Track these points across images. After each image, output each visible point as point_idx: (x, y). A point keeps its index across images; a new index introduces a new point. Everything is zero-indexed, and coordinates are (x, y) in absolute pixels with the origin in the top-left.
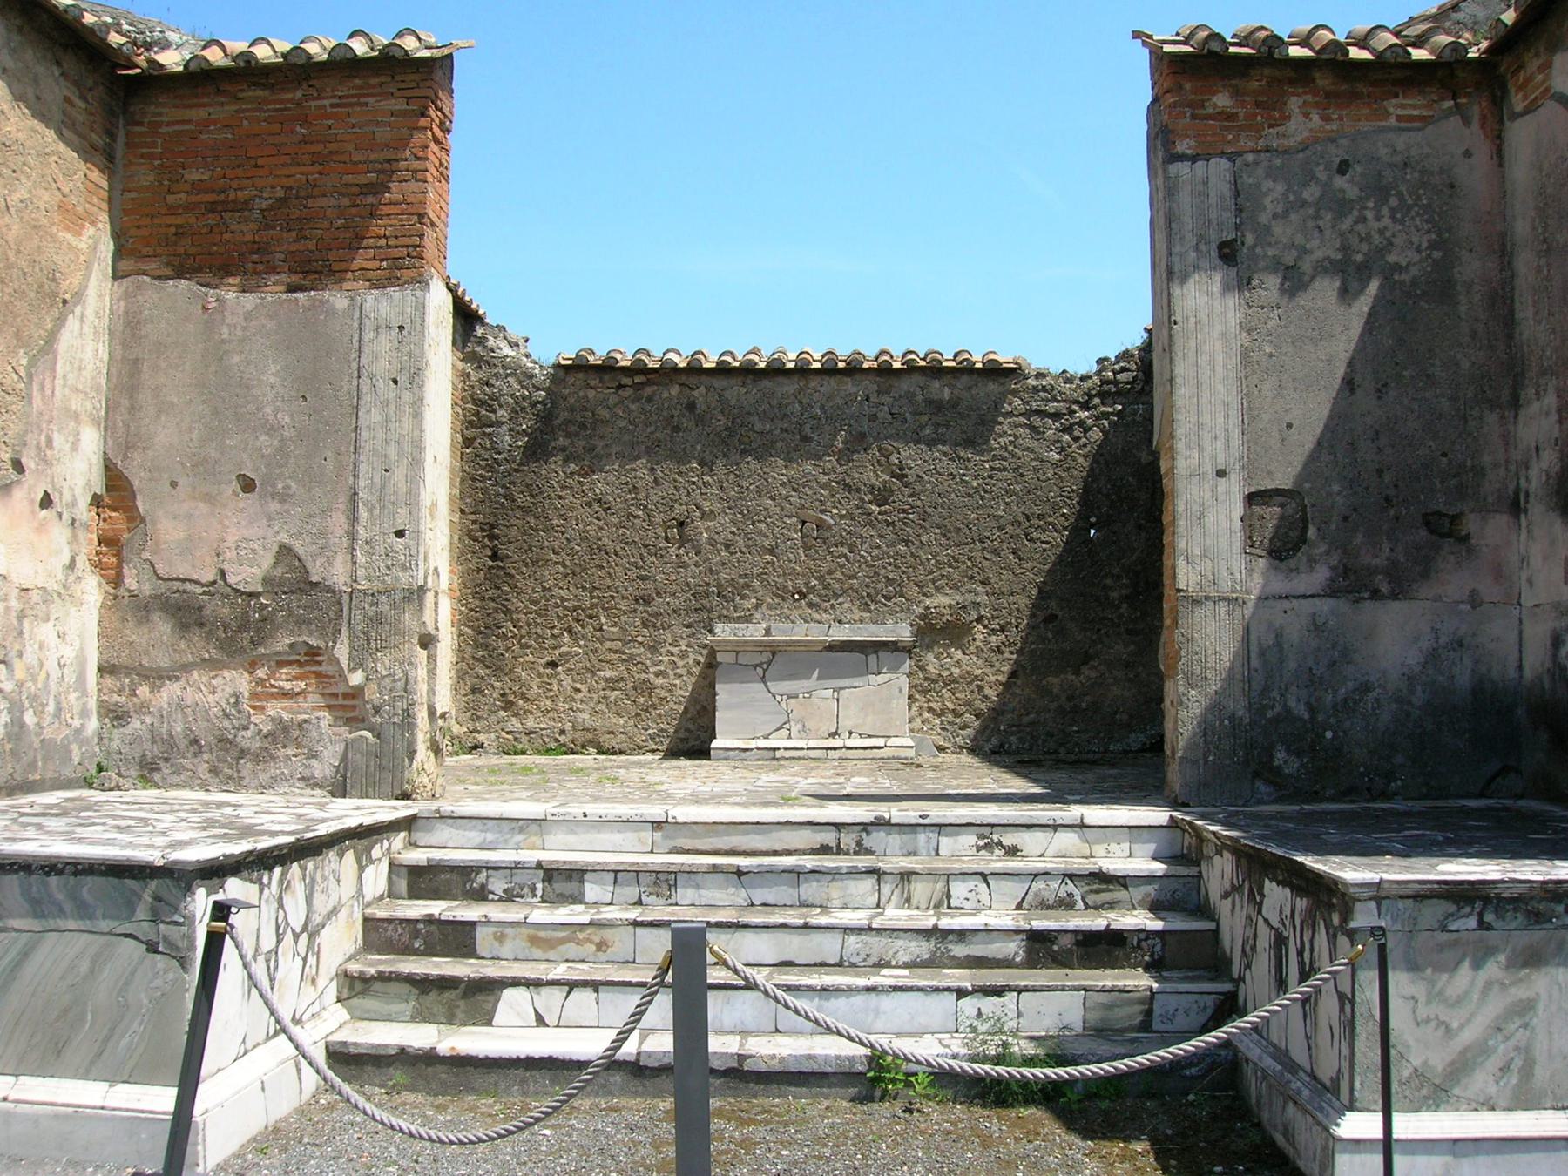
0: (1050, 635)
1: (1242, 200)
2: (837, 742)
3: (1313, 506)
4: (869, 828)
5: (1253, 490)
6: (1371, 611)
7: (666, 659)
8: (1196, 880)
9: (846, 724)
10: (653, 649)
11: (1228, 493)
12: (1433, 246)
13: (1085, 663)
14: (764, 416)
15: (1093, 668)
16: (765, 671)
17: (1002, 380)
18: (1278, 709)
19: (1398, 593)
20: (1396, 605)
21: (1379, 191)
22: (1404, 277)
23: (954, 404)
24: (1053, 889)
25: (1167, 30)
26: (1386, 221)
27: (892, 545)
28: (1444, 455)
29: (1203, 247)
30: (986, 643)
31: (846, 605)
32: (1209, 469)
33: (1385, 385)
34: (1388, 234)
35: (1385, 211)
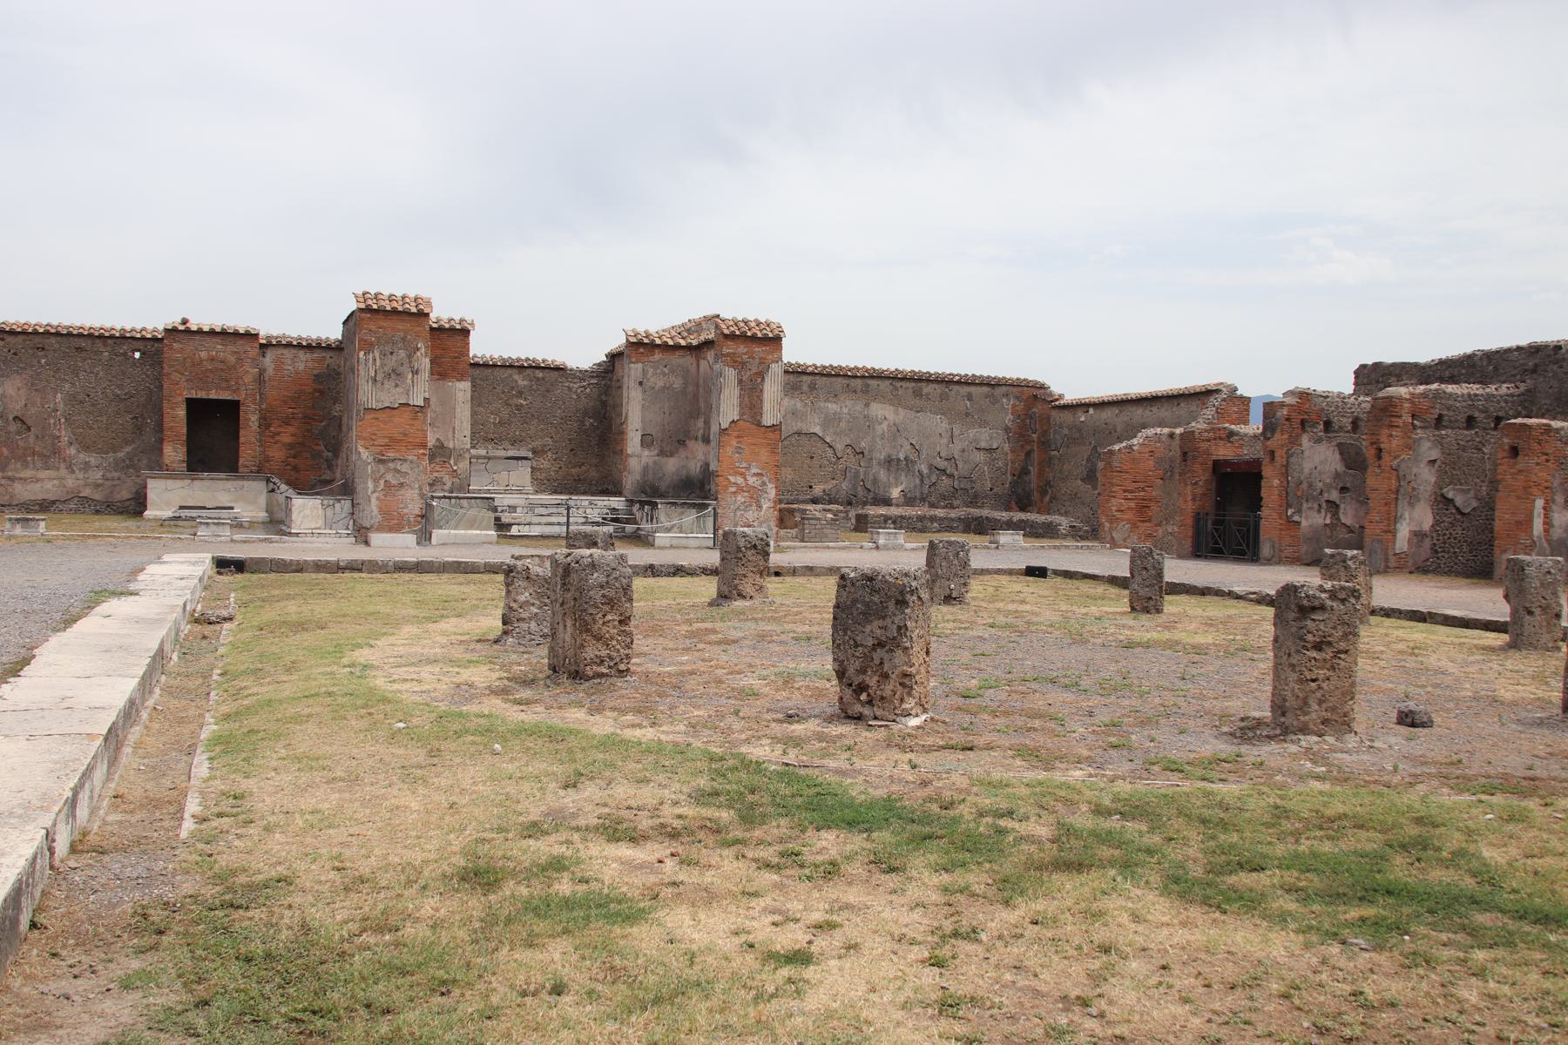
1: (644, 372)
6: (665, 459)
9: (511, 482)
14: (481, 379)
19: (671, 456)
20: (672, 459)
21: (672, 371)
23: (543, 379)
24: (605, 511)
25: (629, 328)
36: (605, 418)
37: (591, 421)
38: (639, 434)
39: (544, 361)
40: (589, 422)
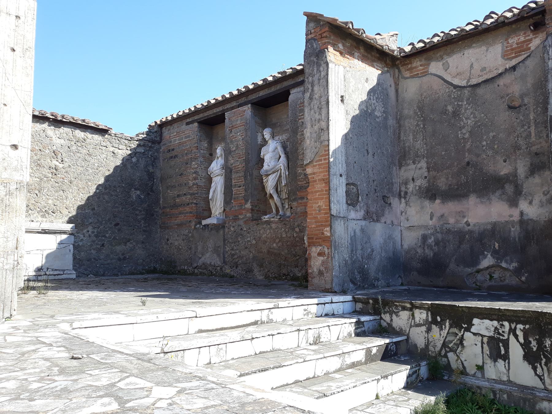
4: (272, 310)
8: (379, 320)
13: (129, 241)
18: (355, 257)
26: (375, 101)
27: (57, 192)
29: (337, 96)
30: (93, 232)
31: (35, 215)
32: (338, 173)
33: (374, 153)
35: (375, 98)
36: (152, 191)
37: (138, 192)
38: (343, 180)
39: (84, 121)
40: (135, 194)
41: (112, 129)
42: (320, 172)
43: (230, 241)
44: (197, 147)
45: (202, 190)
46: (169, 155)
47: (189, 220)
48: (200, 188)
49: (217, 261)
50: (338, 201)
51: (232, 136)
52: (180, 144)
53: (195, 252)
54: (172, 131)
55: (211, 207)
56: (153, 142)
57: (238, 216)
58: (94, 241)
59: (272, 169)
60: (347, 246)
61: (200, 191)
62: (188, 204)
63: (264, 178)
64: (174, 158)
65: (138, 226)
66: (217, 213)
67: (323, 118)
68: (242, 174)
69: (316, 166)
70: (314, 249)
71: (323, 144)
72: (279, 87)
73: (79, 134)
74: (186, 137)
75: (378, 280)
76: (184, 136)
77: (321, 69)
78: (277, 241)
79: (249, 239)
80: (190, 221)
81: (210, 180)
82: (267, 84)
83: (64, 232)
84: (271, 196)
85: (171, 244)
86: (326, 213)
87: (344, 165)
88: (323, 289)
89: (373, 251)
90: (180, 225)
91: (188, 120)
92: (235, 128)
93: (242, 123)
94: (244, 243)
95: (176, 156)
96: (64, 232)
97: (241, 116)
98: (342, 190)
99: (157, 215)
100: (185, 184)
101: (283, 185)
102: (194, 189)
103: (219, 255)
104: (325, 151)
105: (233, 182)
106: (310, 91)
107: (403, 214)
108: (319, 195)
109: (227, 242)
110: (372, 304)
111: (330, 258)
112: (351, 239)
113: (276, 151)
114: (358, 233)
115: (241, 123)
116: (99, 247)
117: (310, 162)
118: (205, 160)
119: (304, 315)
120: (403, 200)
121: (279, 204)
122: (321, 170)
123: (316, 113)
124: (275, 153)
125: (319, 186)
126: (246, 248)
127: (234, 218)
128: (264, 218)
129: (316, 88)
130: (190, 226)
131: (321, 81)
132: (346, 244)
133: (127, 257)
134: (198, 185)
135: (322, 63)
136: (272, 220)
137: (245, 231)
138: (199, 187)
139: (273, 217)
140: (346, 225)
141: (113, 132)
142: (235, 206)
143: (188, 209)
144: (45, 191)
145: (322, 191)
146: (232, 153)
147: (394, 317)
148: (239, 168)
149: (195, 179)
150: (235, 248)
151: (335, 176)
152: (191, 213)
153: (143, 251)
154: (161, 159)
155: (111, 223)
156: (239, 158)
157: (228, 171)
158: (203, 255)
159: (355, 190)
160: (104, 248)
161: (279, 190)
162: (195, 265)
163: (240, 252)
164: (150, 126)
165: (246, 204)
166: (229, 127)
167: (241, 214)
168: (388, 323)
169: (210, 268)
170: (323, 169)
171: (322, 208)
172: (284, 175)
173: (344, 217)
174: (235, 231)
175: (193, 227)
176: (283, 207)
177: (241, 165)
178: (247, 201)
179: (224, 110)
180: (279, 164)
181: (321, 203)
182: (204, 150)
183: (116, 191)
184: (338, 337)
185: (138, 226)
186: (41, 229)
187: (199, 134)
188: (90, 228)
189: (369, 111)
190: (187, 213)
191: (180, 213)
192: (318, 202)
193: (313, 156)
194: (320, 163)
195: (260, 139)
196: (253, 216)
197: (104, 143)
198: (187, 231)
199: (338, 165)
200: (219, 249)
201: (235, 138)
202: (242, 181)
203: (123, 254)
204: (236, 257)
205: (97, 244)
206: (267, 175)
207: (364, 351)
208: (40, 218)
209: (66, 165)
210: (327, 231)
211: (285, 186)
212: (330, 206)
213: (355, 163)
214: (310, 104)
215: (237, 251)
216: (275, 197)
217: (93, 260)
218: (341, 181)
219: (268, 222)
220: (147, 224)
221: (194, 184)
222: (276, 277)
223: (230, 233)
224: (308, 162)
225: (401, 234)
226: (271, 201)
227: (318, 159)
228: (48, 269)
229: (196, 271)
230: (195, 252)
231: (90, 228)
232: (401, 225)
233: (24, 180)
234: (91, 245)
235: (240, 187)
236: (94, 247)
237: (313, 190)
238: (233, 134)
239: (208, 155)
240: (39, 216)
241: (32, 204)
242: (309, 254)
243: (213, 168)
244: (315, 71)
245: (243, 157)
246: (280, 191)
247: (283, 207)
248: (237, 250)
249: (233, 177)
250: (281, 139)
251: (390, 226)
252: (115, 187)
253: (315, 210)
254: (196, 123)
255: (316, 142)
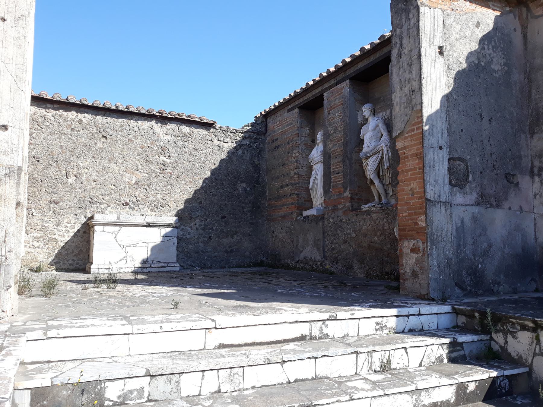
0: (223, 224)
2: (147, 265)
3: (471, 166)
4: (327, 323)
5: (451, 157)
7: (65, 229)
8: (489, 341)
10: (58, 224)
11: (443, 157)
12: (505, 64)
13: (236, 234)
15: (238, 236)
16: (116, 235)
17: (208, 128)
18: (463, 254)
22: (497, 75)
27: (165, 186)
28: (510, 150)
29: (433, 47)
30: (200, 225)
31: (145, 209)
32: (436, 145)
33: (491, 118)
34: (491, 56)
36: (258, 183)
37: (244, 185)
38: (445, 155)
39: (190, 116)
40: (241, 186)
41: (216, 122)
42: (412, 146)
43: (330, 233)
44: (298, 134)
45: (303, 180)
46: (273, 145)
47: (291, 212)
48: (301, 177)
49: (316, 255)
50: (437, 182)
51: (330, 118)
52: (283, 133)
53: (297, 246)
54: (276, 120)
55: (312, 197)
56: (258, 133)
57: (337, 206)
58: (201, 234)
59: (372, 150)
60: (450, 240)
61: (302, 181)
62: (290, 195)
63: (364, 162)
64: (278, 148)
65: (245, 219)
66: (318, 203)
67: (414, 76)
68: (341, 159)
69: (407, 138)
70: (406, 243)
71: (415, 109)
72: (378, 55)
73: (185, 129)
74: (288, 125)
75: (499, 284)
76: (286, 124)
77: (411, 16)
78: (379, 233)
79: (348, 231)
80: (292, 213)
81: (310, 168)
82: (365, 54)
83: (168, 226)
84: (372, 182)
85: (276, 236)
86: (420, 198)
87: (446, 135)
88: (418, 295)
89: (490, 246)
90: (283, 217)
91: (290, 107)
92: (334, 108)
93: (341, 101)
94: (343, 236)
95: (279, 146)
96: (168, 226)
97: (340, 94)
98: (443, 167)
99: (263, 207)
100: (288, 174)
101: (386, 167)
102: (296, 179)
103: (318, 249)
104: (418, 118)
105: (332, 168)
106: (398, 45)
107: (538, 197)
108: (411, 175)
109: (326, 234)
110: (479, 318)
111: (426, 256)
112: (457, 230)
113: (377, 129)
114: (467, 221)
115: (339, 102)
116: (206, 239)
117: (399, 134)
118: (307, 147)
119: (377, 330)
120: (537, 179)
121: (381, 191)
122: (413, 142)
123: (405, 72)
124: (376, 132)
125: (411, 163)
126: (346, 241)
127: (333, 208)
128: (364, 208)
129: (405, 41)
130: (292, 218)
131: (411, 31)
132: (450, 236)
133: (234, 250)
134: (299, 175)
135: (412, 8)
136: (373, 209)
137: (344, 222)
138: (300, 176)
139: (374, 206)
140: (448, 213)
141: (218, 125)
142: (334, 195)
143: (290, 200)
144: (154, 186)
145: (415, 169)
146: (331, 137)
147: (510, 338)
148: (337, 152)
149: (296, 168)
150: (335, 241)
151: (432, 150)
152: (293, 204)
153: (250, 244)
154: (267, 150)
155: (218, 216)
156: (338, 141)
157: (327, 156)
158: (304, 248)
159: (463, 166)
160: (212, 241)
161: (381, 174)
162: (297, 259)
163: (340, 246)
164: (256, 117)
165: (344, 192)
166: (328, 109)
167: (340, 204)
168: (501, 347)
169: (311, 263)
170: (416, 141)
171: (415, 191)
172: (387, 156)
173: (446, 202)
174: (334, 223)
175: (295, 219)
176: (387, 194)
177: (340, 149)
178: (345, 189)
179: (322, 90)
180: (380, 144)
181: (414, 185)
182: (305, 137)
183: (222, 184)
184: (421, 362)
185: (245, 219)
186: (145, 222)
187: (299, 120)
188: (197, 221)
189: (483, 64)
190: (289, 204)
191: (283, 205)
192: (410, 184)
193: (403, 126)
194: (412, 133)
195: (360, 119)
196: (352, 206)
197: (210, 137)
198: (290, 223)
199: (435, 135)
200: (319, 243)
201: (334, 119)
202: (341, 167)
203: (230, 247)
204: (336, 251)
205: (205, 237)
206: (367, 158)
207: (454, 387)
208: (149, 212)
209: (173, 160)
210: (421, 220)
211: (388, 168)
212: (424, 187)
213: (462, 131)
214: (398, 62)
215: (337, 245)
216: (376, 182)
217: (200, 252)
218: (440, 155)
219: (368, 212)
220: (253, 217)
221: (295, 174)
222: (377, 276)
223: (330, 225)
224: (397, 134)
225: (535, 224)
226: (372, 187)
227: (409, 129)
228: (153, 261)
229: (298, 265)
230: (297, 246)
231: (197, 221)
232: (535, 211)
233: (15, 165)
234: (199, 238)
235: (339, 173)
236: (202, 239)
237: (404, 169)
238: (332, 115)
239: (310, 142)
240: (149, 210)
241: (142, 199)
242: (401, 250)
243: (313, 155)
244: (404, 20)
245: (341, 140)
246: (383, 175)
247: (387, 194)
248: (337, 243)
249: (332, 163)
250: (384, 115)
251: (518, 213)
252: (221, 180)
253: (407, 194)
254: (297, 109)
255: (406, 108)
